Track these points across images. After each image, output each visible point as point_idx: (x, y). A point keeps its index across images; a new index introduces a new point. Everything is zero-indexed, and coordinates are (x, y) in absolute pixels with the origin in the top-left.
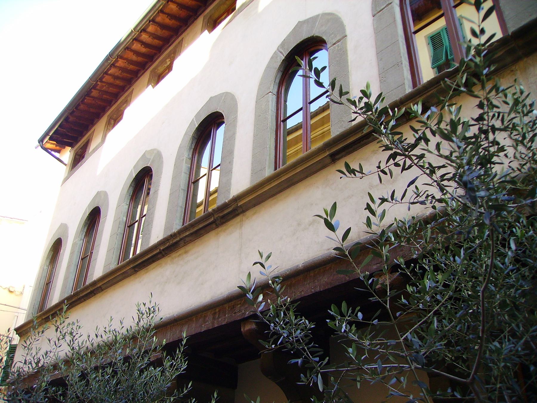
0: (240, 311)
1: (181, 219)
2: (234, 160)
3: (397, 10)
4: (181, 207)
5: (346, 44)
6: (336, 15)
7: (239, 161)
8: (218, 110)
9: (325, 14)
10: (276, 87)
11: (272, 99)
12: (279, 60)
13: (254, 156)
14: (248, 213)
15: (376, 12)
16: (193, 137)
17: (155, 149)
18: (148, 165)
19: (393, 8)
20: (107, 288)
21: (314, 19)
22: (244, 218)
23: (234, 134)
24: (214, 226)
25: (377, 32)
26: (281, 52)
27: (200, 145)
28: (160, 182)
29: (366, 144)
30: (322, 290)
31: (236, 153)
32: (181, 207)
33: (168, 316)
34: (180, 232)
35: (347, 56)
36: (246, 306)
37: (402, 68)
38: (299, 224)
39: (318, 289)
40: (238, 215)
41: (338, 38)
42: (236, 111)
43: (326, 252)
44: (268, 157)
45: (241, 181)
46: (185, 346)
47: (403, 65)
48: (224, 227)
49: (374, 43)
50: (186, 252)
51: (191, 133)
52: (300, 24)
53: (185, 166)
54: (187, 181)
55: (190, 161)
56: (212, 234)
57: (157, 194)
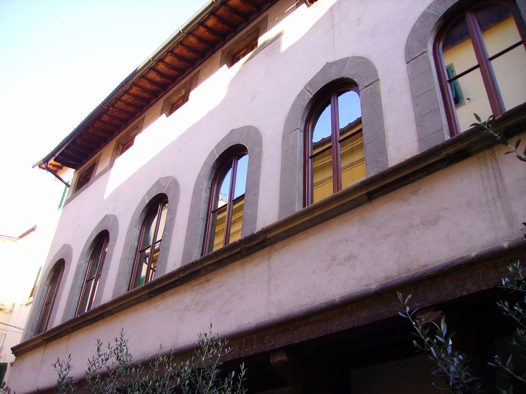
0: (269, 342)
1: (200, 247)
2: (260, 193)
3: (431, 58)
4: (200, 235)
5: (378, 87)
6: (367, 59)
7: (267, 192)
8: (240, 143)
9: (354, 58)
10: (303, 124)
11: (300, 135)
12: (307, 98)
13: (282, 190)
14: (277, 246)
15: (410, 60)
16: (213, 168)
17: (170, 177)
18: (163, 192)
19: (427, 56)
20: (117, 312)
21: (343, 62)
22: (272, 250)
23: (259, 167)
24: (239, 256)
25: (412, 78)
26: (308, 91)
27: (218, 176)
28: (176, 209)
29: (405, 185)
30: (360, 325)
31: (261, 185)
32: (200, 235)
33: (188, 343)
34: (201, 261)
35: (381, 99)
36: (276, 338)
37: (440, 114)
38: (334, 259)
39: (356, 324)
40: (266, 247)
41: (370, 81)
42: (261, 145)
43: (364, 288)
44: (297, 193)
45: (267, 213)
46: (244, 377)
47: (441, 112)
48: (249, 258)
49: (409, 89)
50: (208, 281)
51: (211, 164)
52: (329, 66)
53: (205, 195)
54: (206, 210)
55: (209, 191)
56: (238, 263)
57: (174, 220)
